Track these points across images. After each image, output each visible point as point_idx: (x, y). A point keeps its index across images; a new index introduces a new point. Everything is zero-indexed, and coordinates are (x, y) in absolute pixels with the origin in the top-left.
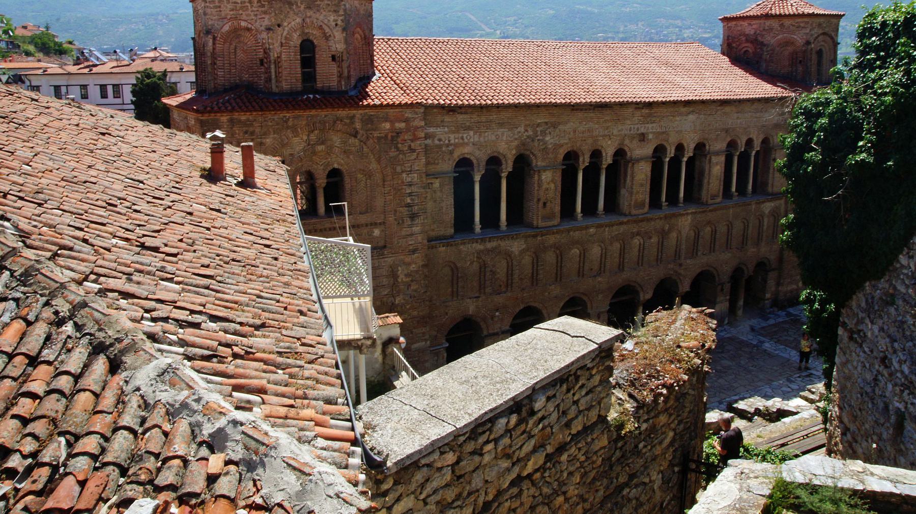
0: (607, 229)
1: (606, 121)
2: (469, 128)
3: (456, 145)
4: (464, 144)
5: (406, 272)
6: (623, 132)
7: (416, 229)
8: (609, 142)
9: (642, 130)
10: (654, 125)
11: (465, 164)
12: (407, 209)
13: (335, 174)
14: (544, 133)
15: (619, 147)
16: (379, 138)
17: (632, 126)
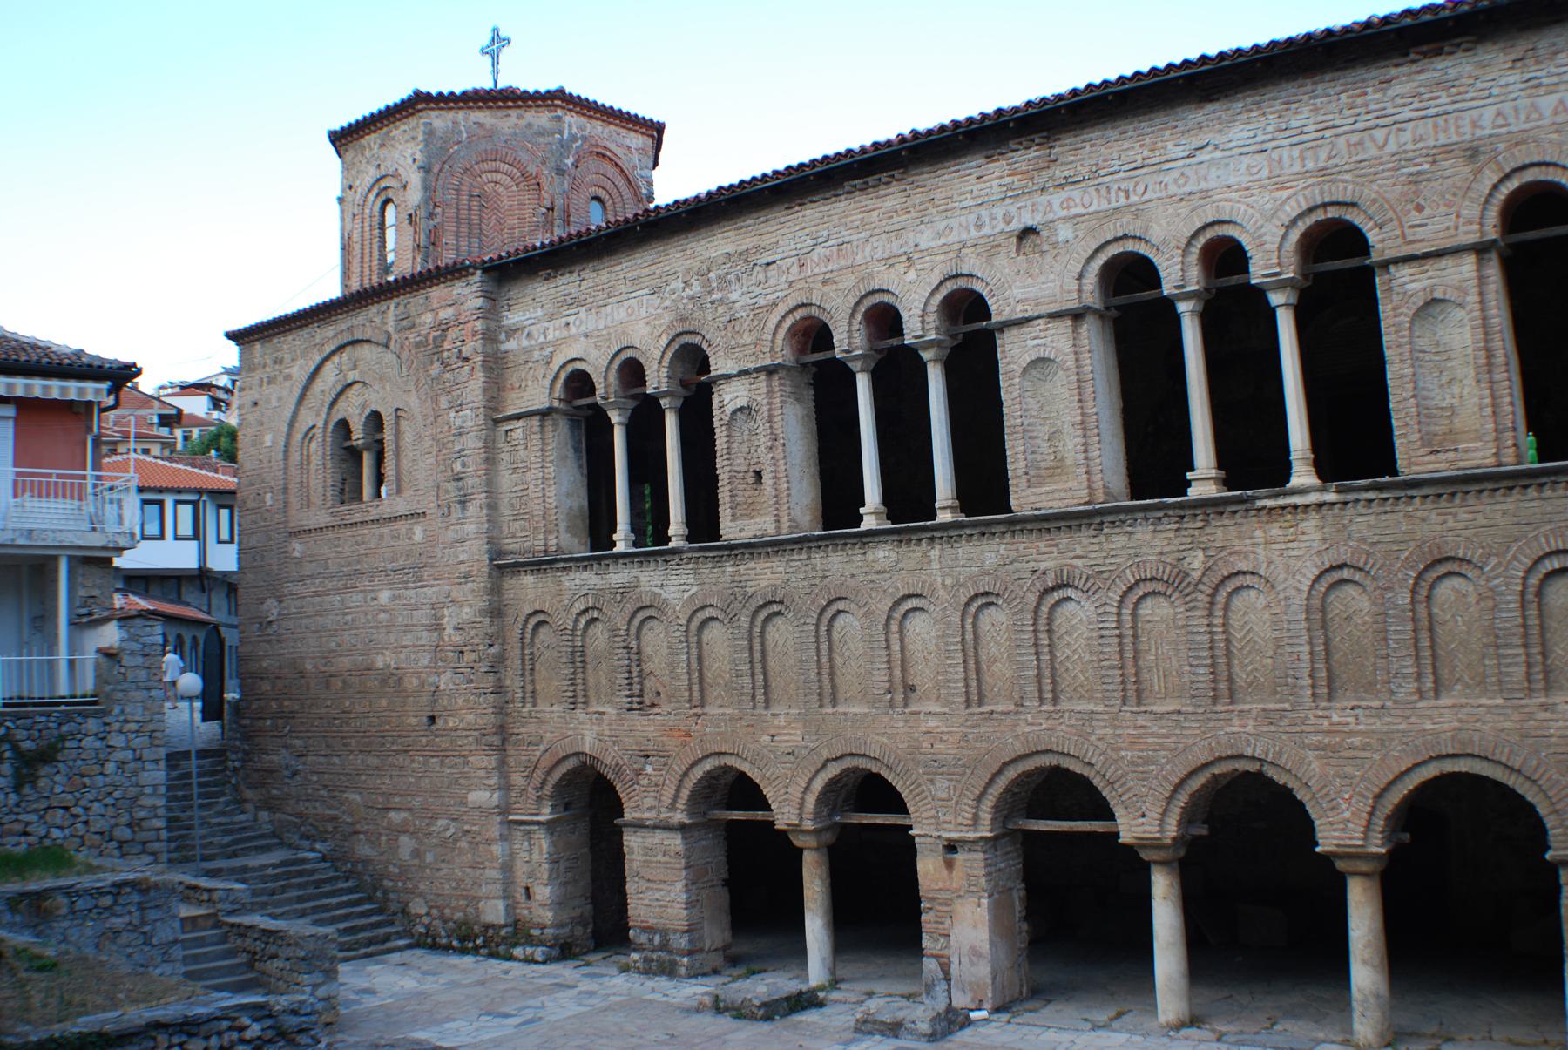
0: (935, 553)
1: (889, 214)
2: (577, 303)
3: (556, 344)
4: (566, 340)
5: (455, 621)
6: (953, 238)
7: (470, 528)
8: (912, 275)
9: (1028, 220)
10: (1074, 193)
11: (579, 383)
12: (455, 484)
13: (376, 420)
14: (724, 282)
15: (950, 287)
16: (418, 345)
17: (984, 213)
